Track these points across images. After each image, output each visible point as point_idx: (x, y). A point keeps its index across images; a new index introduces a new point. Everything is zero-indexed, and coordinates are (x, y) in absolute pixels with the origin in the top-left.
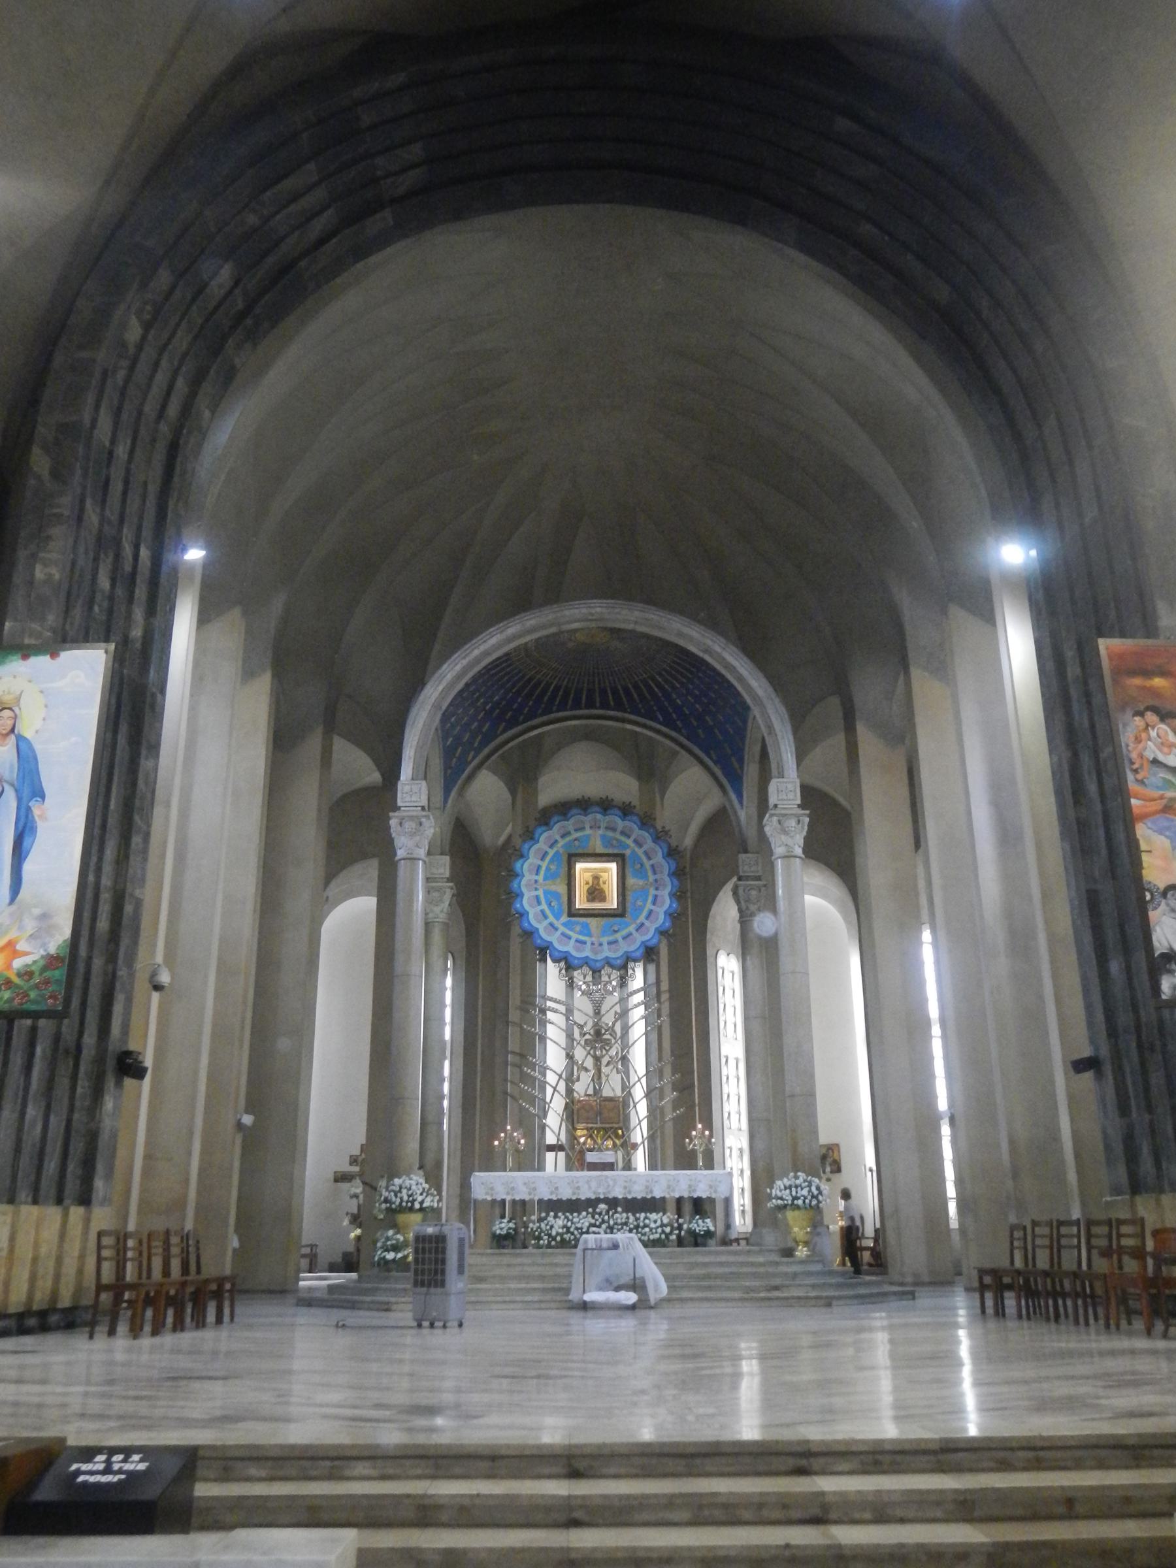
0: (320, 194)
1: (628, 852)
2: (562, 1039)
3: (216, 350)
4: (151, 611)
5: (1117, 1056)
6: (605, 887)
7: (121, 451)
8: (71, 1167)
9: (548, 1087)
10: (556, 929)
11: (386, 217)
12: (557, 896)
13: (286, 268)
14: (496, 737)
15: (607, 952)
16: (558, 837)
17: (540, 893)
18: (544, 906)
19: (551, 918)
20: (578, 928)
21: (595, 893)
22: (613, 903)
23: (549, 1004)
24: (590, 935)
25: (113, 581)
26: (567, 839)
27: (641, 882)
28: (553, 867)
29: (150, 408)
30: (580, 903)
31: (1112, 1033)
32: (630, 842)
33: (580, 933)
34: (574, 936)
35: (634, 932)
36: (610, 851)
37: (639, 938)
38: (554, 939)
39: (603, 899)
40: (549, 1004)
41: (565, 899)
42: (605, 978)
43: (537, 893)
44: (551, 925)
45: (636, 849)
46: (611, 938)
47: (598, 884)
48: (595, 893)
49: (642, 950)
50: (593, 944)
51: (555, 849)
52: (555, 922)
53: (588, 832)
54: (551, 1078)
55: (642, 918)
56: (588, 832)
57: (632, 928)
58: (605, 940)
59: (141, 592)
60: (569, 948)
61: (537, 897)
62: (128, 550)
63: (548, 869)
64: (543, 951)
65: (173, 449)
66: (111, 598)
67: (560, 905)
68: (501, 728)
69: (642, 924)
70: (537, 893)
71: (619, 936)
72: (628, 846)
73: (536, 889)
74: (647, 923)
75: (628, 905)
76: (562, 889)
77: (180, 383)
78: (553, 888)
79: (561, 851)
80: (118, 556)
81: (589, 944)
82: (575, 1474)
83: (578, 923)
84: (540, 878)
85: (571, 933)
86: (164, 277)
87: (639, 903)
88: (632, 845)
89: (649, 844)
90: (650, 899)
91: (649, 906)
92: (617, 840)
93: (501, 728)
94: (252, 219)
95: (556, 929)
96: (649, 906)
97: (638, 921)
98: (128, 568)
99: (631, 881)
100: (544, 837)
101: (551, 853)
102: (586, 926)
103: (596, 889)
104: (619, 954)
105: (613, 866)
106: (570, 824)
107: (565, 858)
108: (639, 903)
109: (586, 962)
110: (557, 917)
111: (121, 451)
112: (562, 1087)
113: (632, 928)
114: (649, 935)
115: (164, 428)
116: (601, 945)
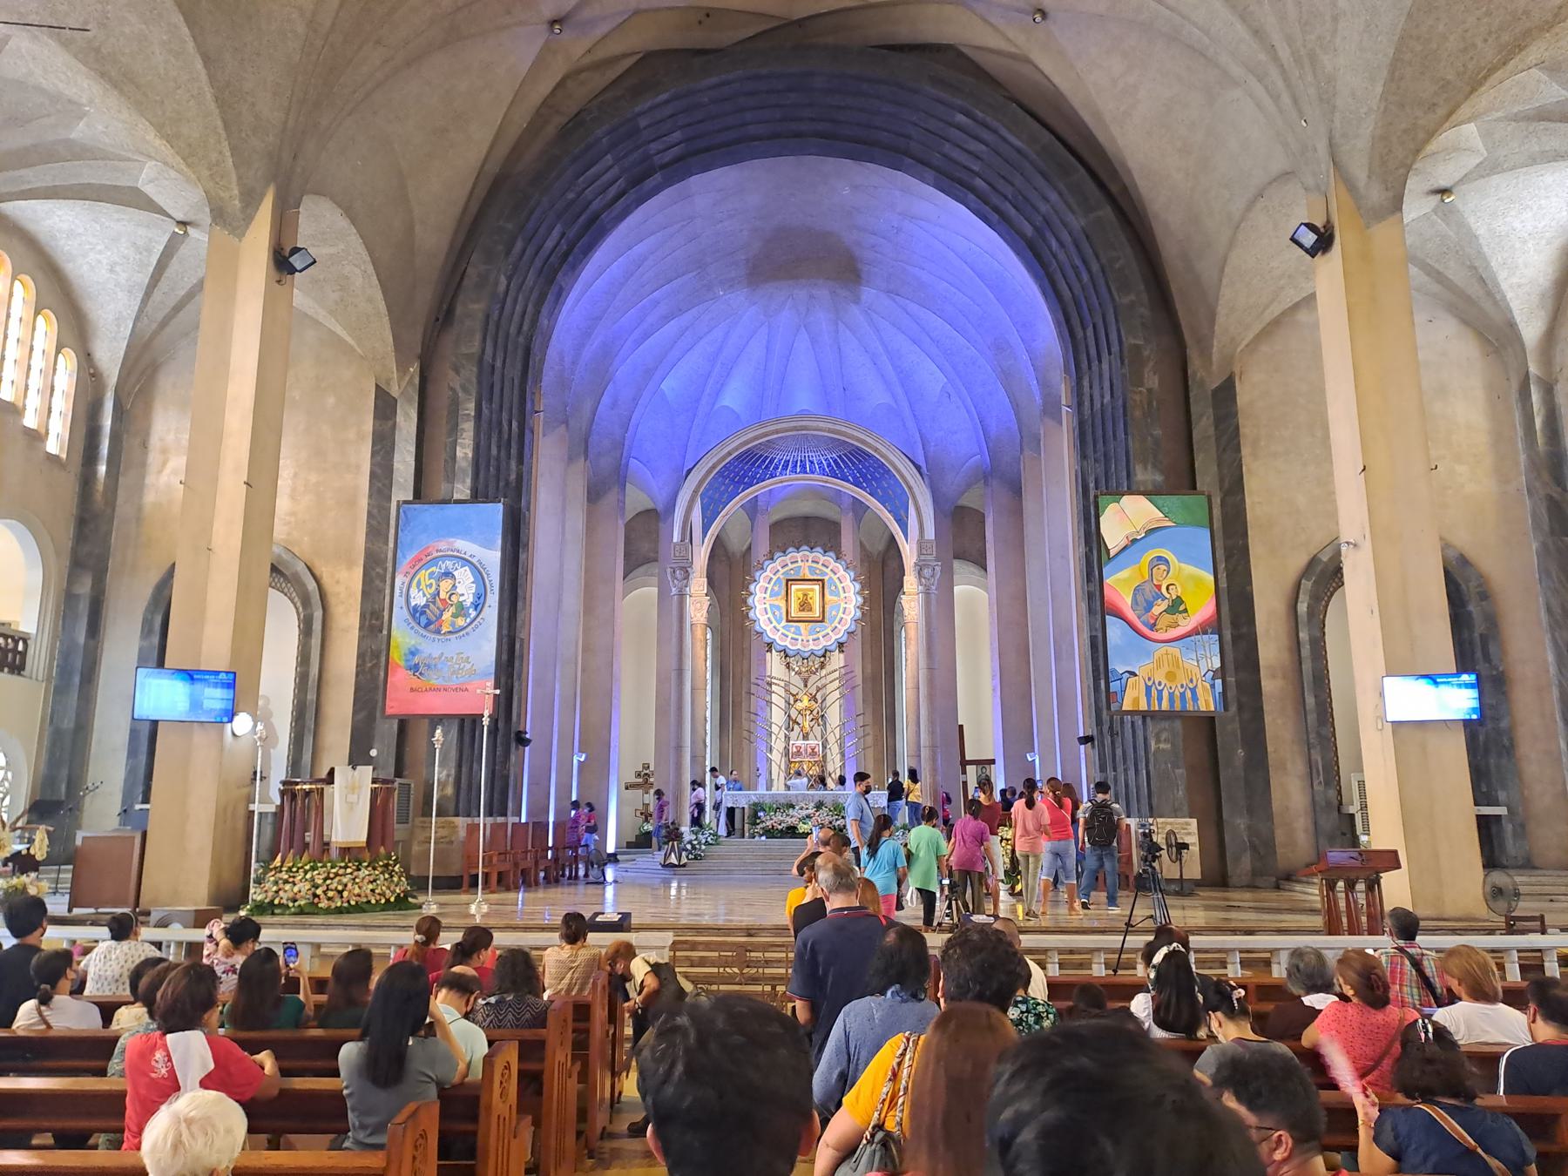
0: (615, 170)
2: (782, 704)
3: (551, 281)
4: (520, 461)
5: (1101, 732)
7: (499, 364)
8: (496, 795)
11: (657, 178)
13: (595, 218)
21: (805, 605)
22: (817, 613)
25: (499, 447)
29: (513, 330)
30: (794, 613)
31: (1099, 722)
38: (777, 637)
48: (805, 605)
54: (775, 729)
55: (836, 623)
59: (514, 451)
60: (787, 643)
62: (505, 424)
64: (770, 646)
65: (528, 352)
66: (498, 459)
76: (782, 604)
77: (530, 307)
80: (500, 432)
82: (750, 935)
86: (519, 245)
89: (842, 572)
94: (571, 196)
98: (506, 436)
99: (828, 597)
100: (770, 567)
102: (798, 628)
105: (817, 588)
106: (787, 559)
109: (798, 652)
111: (499, 364)
112: (782, 736)
114: (840, 635)
115: (521, 339)
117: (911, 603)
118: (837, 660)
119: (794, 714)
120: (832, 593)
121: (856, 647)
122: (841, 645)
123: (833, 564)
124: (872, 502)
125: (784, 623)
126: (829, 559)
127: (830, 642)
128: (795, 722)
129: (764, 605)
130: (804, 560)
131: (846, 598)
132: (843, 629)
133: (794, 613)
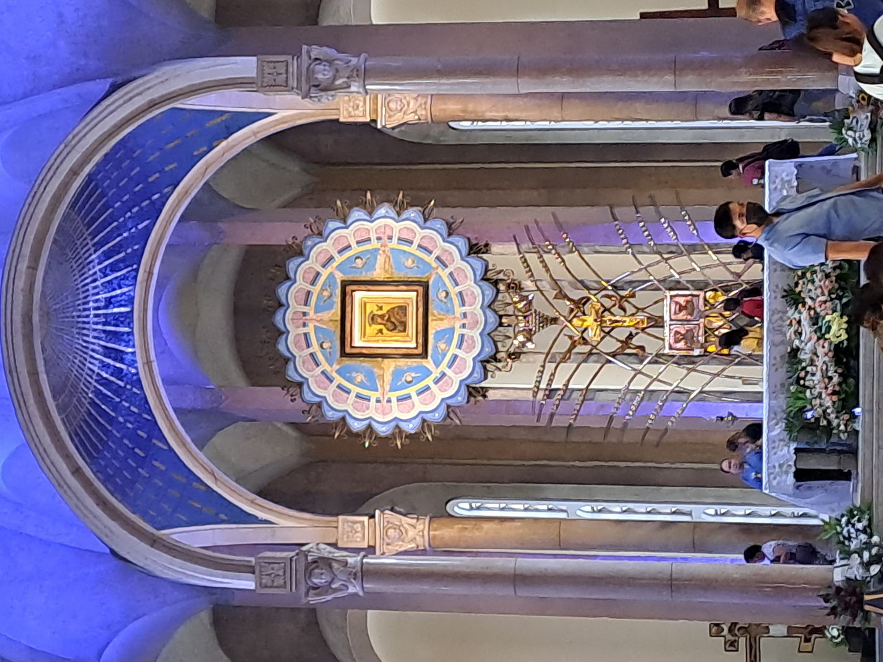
1: (339, 277)
2: (591, 367)
6: (386, 309)
9: (651, 388)
10: (444, 375)
12: (398, 374)
14: (171, 449)
15: (475, 308)
16: (318, 371)
17: (394, 396)
18: (412, 390)
19: (429, 381)
20: (443, 346)
21: (394, 321)
22: (410, 296)
23: (543, 386)
24: (453, 330)
26: (320, 357)
27: (380, 259)
28: (360, 378)
32: (325, 273)
33: (449, 343)
34: (453, 350)
35: (448, 271)
36: (338, 300)
37: (458, 263)
38: (456, 378)
39: (403, 309)
40: (543, 386)
41: (402, 362)
42: (510, 310)
43: (394, 400)
44: (436, 382)
45: (335, 264)
46: (456, 301)
47: (382, 316)
48: (394, 321)
49: (472, 260)
50: (464, 326)
51: (334, 375)
52: (433, 377)
53: (310, 329)
54: (640, 384)
55: (431, 259)
56: (310, 329)
57: (444, 273)
58: (459, 310)
60: (468, 359)
61: (399, 399)
63: (361, 385)
64: (474, 392)
67: (411, 369)
68: (160, 445)
69: (438, 258)
70: (394, 400)
71: (454, 291)
72: (331, 275)
73: (389, 401)
74: (437, 252)
75: (412, 276)
78: (388, 378)
79: (336, 367)
81: (464, 331)
83: (436, 347)
84: (374, 395)
85: (449, 356)
87: (409, 263)
88: (329, 270)
90: (406, 248)
91: (413, 249)
92: (322, 290)
93: (160, 445)
95: (444, 375)
96: (413, 249)
97: (434, 265)
99: (378, 274)
100: (316, 388)
101: (338, 380)
102: (440, 334)
103: (389, 320)
104: (477, 291)
105: (359, 296)
106: (300, 355)
107: (348, 362)
108: (409, 263)
109: (489, 336)
110: (430, 373)
113: (444, 273)
114: (454, 250)
116: (465, 315)
117: (397, 105)
118: (504, 256)
119: (610, 345)
120: (370, 265)
121: (481, 218)
122: (475, 249)
123: (312, 263)
124: (193, 181)
125: (429, 363)
126: (300, 271)
127: (467, 271)
128: (626, 343)
129: (393, 402)
130: (303, 324)
131: (383, 236)
132: (441, 246)
133: (409, 341)
